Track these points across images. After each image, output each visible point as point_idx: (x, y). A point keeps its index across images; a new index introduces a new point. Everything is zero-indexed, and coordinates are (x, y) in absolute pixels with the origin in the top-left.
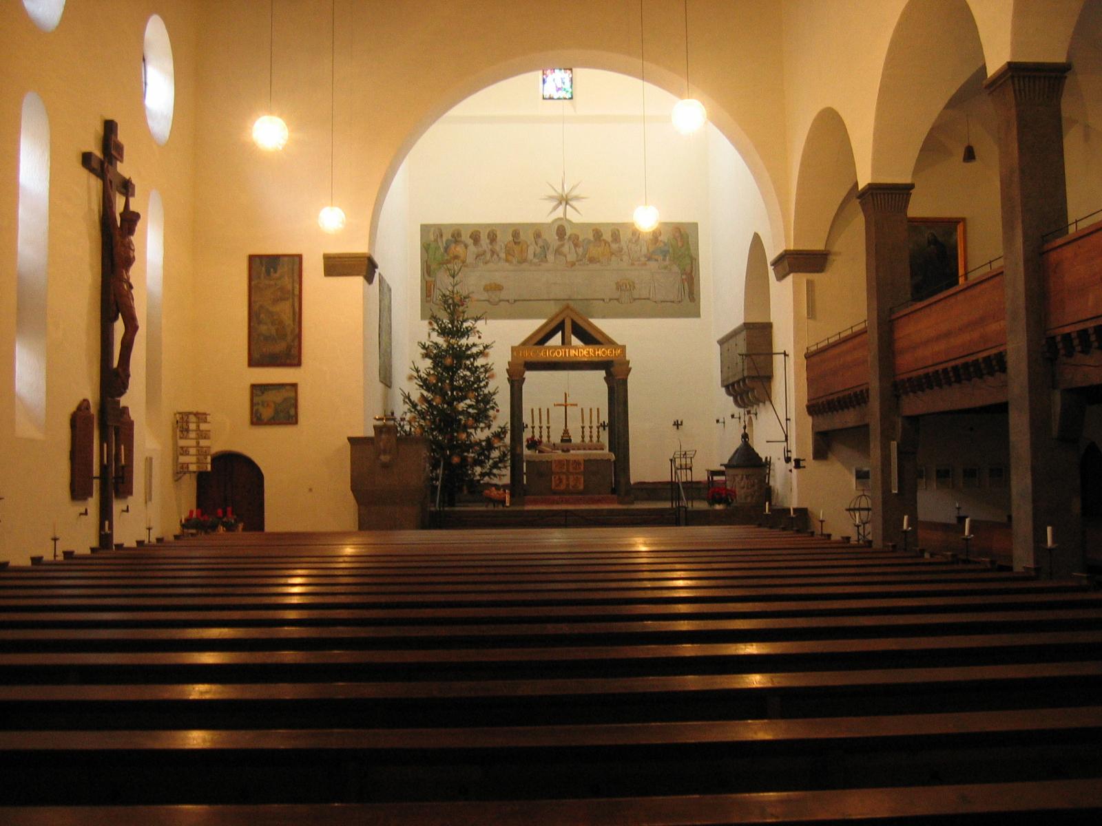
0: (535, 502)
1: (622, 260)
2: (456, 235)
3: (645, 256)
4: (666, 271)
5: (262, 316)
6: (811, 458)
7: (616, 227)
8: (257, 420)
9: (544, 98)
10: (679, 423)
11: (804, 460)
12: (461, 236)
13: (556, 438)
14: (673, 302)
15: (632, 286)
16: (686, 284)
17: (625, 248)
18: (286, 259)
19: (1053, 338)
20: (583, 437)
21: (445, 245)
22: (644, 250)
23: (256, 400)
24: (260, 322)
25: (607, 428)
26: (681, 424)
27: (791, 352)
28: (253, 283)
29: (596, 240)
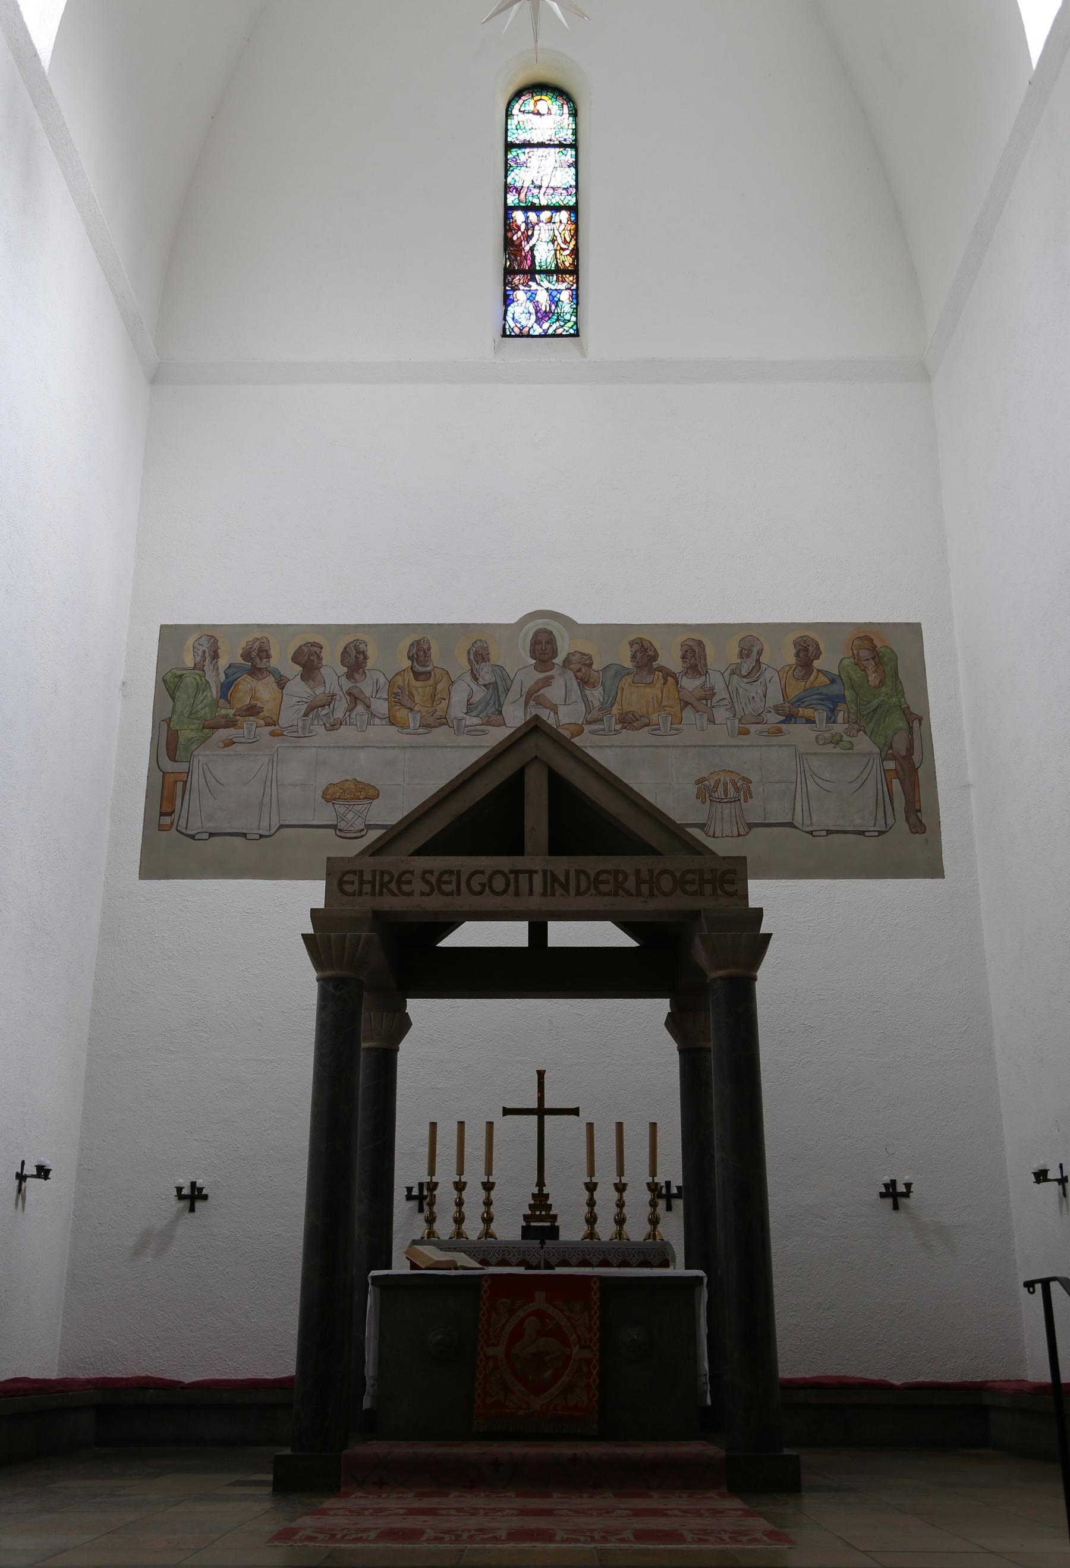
1: (712, 721)
2: (254, 654)
3: (777, 709)
4: (838, 750)
7: (697, 636)
9: (504, 335)
10: (901, 1188)
12: (268, 657)
14: (863, 833)
15: (743, 789)
16: (896, 784)
17: (721, 692)
20: (591, 1220)
21: (222, 678)
22: (775, 696)
25: (679, 1204)
26: (906, 1195)
29: (639, 667)
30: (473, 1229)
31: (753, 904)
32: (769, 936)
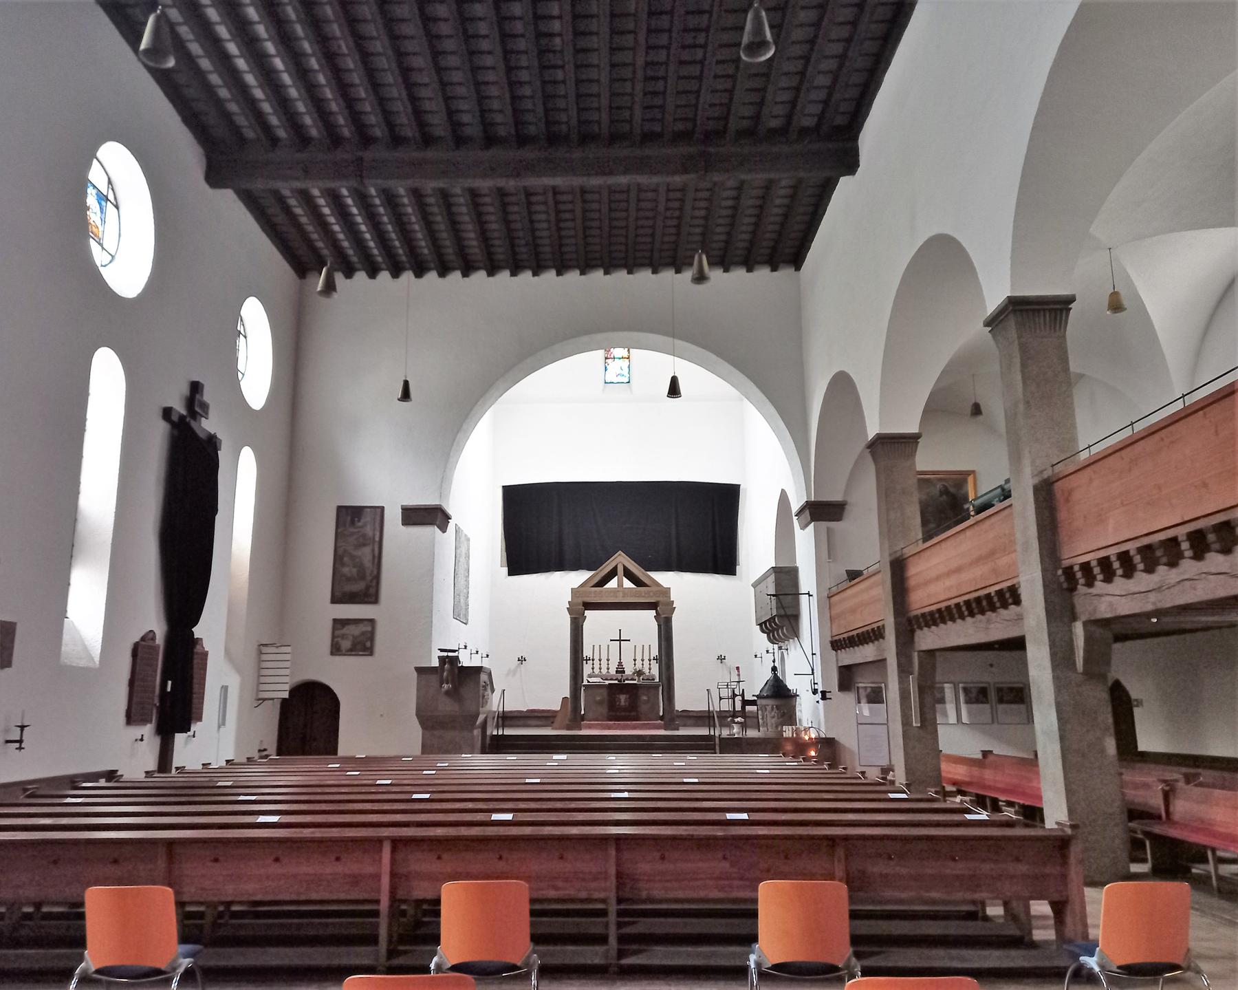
0: (590, 727)
5: (346, 559)
6: (837, 690)
8: (336, 650)
9: (605, 383)
10: (723, 657)
11: (830, 692)
13: (613, 671)
18: (369, 510)
19: (1071, 567)
23: (337, 633)
24: (343, 565)
26: (724, 659)
27: (814, 592)
28: (339, 530)
30: (604, 671)
31: (672, 600)
32: (675, 608)
